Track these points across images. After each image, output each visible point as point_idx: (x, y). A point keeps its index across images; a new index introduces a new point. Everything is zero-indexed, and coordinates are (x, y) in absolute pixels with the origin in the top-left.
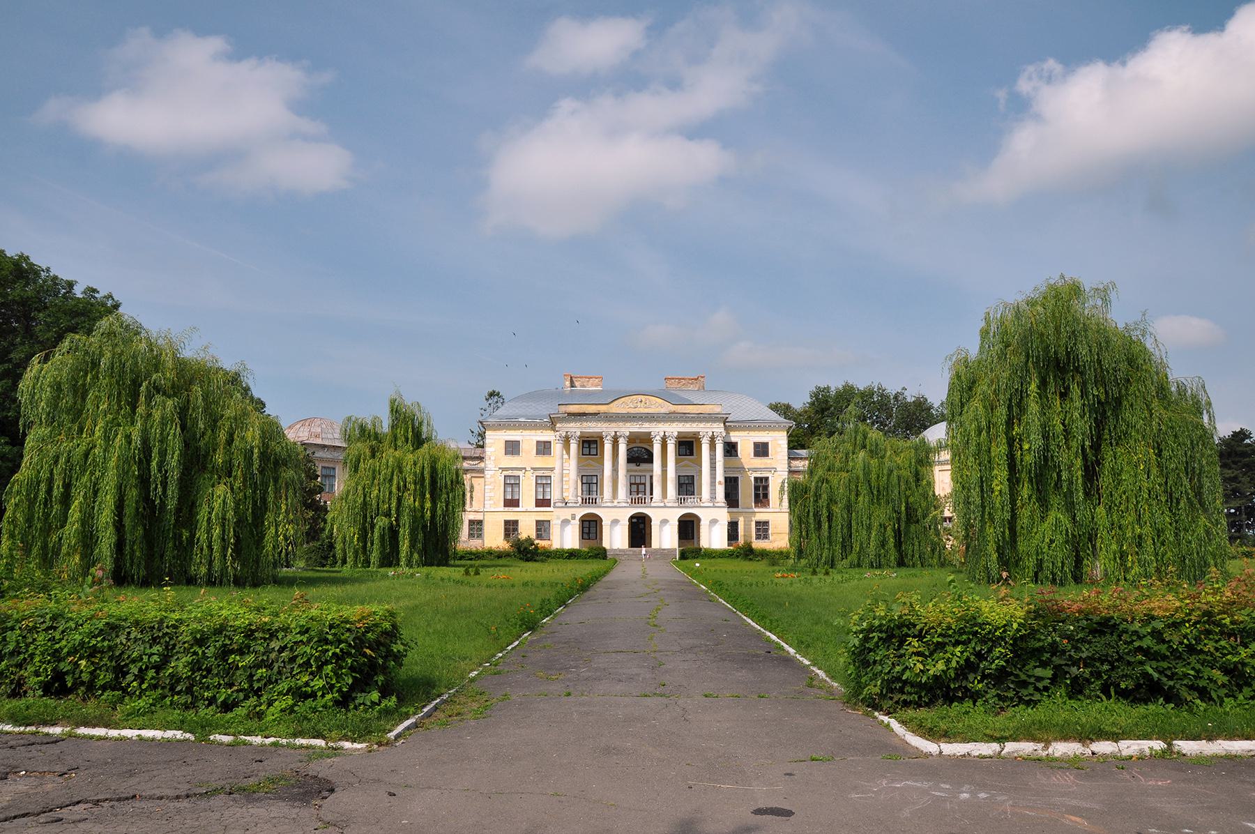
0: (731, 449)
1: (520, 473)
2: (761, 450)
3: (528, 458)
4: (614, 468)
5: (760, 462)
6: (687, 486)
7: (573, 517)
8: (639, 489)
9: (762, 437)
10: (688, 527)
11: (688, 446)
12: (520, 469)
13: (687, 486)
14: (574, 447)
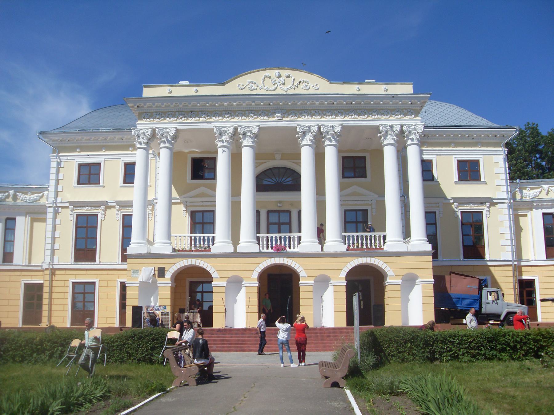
0: (426, 168)
1: (100, 212)
2: (469, 171)
3: (111, 186)
4: (234, 194)
5: (470, 190)
6: (360, 219)
7: (161, 272)
8: (278, 221)
9: (468, 154)
10: (366, 288)
11: (357, 166)
12: (97, 204)
13: (360, 219)
14: (165, 154)
